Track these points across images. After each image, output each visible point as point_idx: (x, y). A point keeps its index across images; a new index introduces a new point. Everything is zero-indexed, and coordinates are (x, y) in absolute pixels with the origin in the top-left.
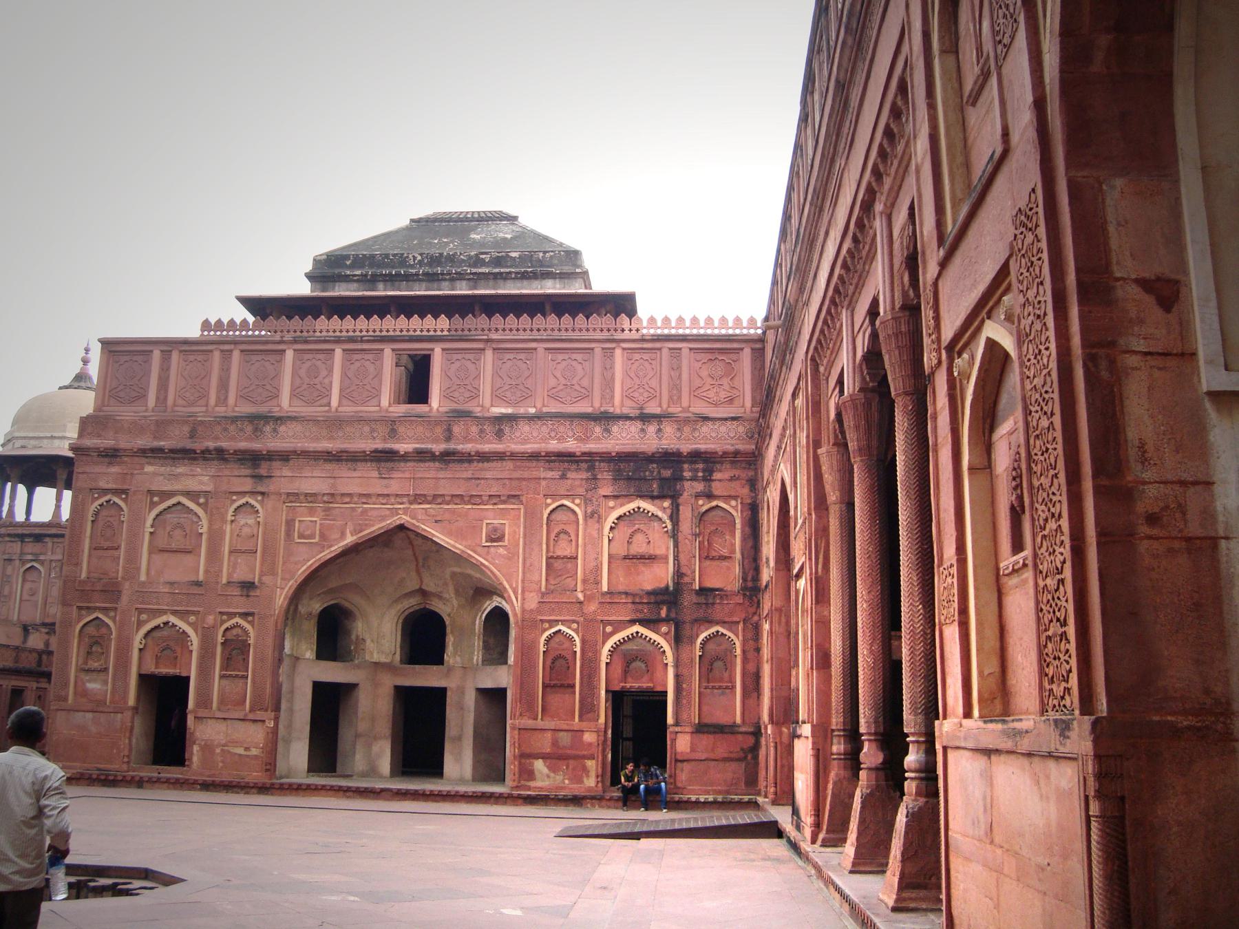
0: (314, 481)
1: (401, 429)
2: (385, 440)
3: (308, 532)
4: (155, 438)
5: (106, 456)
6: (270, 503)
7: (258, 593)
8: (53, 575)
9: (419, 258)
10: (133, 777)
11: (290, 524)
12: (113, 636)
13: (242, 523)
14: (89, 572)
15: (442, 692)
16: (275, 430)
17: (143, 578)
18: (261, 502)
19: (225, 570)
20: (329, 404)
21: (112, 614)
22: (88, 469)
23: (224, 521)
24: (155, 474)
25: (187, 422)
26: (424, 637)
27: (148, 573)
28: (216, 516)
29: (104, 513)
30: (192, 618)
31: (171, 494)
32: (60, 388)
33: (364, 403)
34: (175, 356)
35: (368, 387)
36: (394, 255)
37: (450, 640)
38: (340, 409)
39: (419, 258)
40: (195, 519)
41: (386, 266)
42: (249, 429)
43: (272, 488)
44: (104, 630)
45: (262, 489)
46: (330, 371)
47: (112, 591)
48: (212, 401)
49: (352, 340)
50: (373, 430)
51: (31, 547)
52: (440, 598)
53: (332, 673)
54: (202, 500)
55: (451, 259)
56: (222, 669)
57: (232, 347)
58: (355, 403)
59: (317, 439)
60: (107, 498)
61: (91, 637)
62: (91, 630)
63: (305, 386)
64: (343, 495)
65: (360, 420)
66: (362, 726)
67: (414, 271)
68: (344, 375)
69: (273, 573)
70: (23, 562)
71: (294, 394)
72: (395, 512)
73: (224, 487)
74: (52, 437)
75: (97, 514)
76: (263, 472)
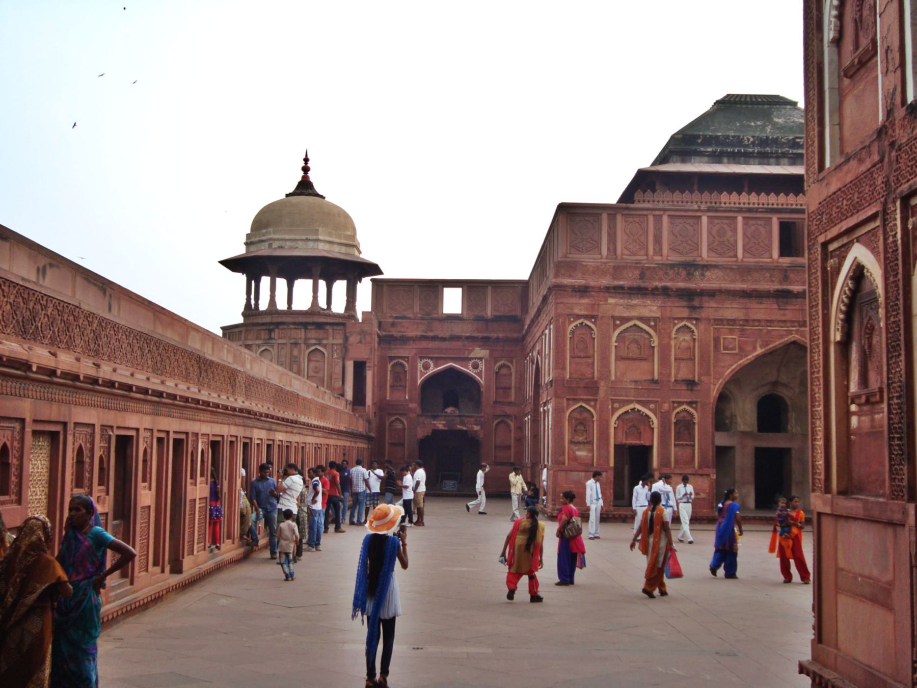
0: (732, 311)
1: (792, 276)
2: (781, 283)
3: (731, 346)
4: (614, 278)
5: (579, 291)
6: (702, 326)
7: (699, 388)
8: (335, 356)
9: (752, 140)
10: (620, 515)
11: (717, 340)
12: (595, 419)
13: (681, 339)
14: (571, 374)
15: (787, 451)
16: (702, 275)
17: (613, 378)
18: (696, 325)
19: (673, 371)
20: (736, 256)
21: (592, 403)
22: (565, 300)
23: (670, 337)
24: (616, 305)
25: (637, 268)
26: (772, 414)
27: (616, 375)
28: (664, 335)
29: (578, 332)
30: (652, 406)
31: (628, 319)
32: (287, 195)
33: (760, 256)
34: (619, 218)
35: (762, 244)
36: (733, 137)
37: (792, 416)
38: (745, 260)
39: (752, 140)
40: (647, 336)
41: (729, 145)
42: (684, 273)
43: (703, 315)
44: (585, 415)
45: (696, 316)
46: (735, 231)
47: (592, 387)
48: (651, 252)
49: (750, 210)
50: (771, 276)
51: (313, 334)
52: (785, 385)
53: (722, 440)
54: (652, 324)
55: (775, 141)
56: (675, 440)
57: (662, 213)
58: (754, 256)
59: (732, 281)
60: (581, 321)
61: (576, 419)
62: (575, 415)
63: (716, 243)
64: (754, 320)
65: (761, 268)
66: (738, 476)
67: (751, 150)
68: (745, 234)
69: (708, 374)
70: (308, 346)
71: (710, 249)
72: (789, 332)
73: (668, 314)
74: (307, 240)
75: (573, 332)
76: (696, 303)
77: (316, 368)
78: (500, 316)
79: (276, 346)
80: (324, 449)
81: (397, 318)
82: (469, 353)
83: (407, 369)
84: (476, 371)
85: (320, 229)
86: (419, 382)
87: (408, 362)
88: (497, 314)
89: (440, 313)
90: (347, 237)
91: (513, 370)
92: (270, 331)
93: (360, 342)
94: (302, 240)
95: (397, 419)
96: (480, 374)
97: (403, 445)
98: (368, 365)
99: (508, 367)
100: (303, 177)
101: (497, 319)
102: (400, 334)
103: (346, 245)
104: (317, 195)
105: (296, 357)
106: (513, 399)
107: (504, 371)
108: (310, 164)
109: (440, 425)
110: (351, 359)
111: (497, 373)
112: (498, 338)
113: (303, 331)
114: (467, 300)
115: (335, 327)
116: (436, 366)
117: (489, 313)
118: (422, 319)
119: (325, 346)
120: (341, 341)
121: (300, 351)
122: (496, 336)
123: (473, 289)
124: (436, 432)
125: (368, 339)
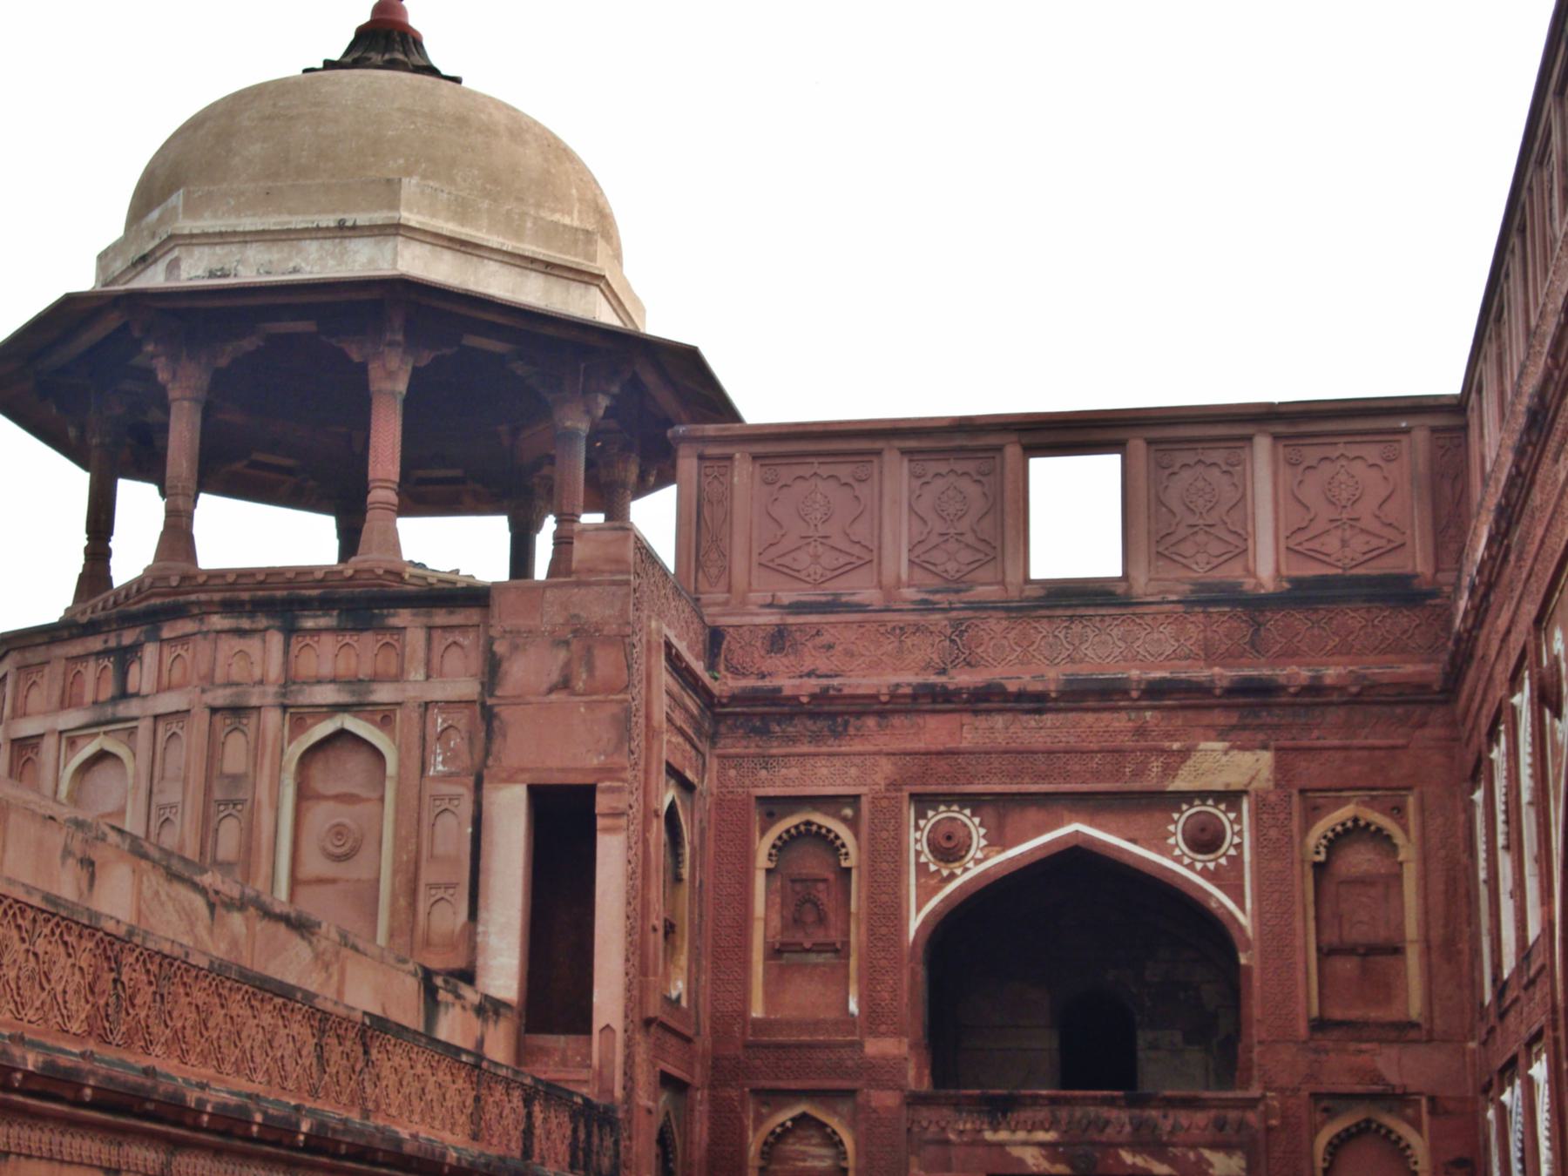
8: (438, 767)
51: (328, 655)
70: (299, 718)
77: (339, 831)
78: (1323, 581)
79: (144, 727)
81: (798, 608)
82: (1170, 771)
84: (1209, 861)
85: (410, 185)
86: (914, 923)
87: (853, 824)
88: (1312, 570)
89: (1013, 577)
90: (553, 232)
91: (1408, 852)
92: (125, 657)
94: (316, 233)
95: (802, 1120)
96: (1229, 879)
98: (602, 803)
99: (1380, 837)
101: (1305, 595)
102: (813, 685)
103: (549, 268)
104: (432, 71)
105: (236, 780)
106: (1415, 1007)
107: (1359, 860)
110: (510, 779)
112: (1315, 688)
113: (276, 640)
115: (441, 617)
116: (998, 840)
117: (1265, 568)
118: (926, 607)
119: (385, 716)
120: (467, 688)
121: (256, 754)
122: (1305, 675)
125: (606, 662)
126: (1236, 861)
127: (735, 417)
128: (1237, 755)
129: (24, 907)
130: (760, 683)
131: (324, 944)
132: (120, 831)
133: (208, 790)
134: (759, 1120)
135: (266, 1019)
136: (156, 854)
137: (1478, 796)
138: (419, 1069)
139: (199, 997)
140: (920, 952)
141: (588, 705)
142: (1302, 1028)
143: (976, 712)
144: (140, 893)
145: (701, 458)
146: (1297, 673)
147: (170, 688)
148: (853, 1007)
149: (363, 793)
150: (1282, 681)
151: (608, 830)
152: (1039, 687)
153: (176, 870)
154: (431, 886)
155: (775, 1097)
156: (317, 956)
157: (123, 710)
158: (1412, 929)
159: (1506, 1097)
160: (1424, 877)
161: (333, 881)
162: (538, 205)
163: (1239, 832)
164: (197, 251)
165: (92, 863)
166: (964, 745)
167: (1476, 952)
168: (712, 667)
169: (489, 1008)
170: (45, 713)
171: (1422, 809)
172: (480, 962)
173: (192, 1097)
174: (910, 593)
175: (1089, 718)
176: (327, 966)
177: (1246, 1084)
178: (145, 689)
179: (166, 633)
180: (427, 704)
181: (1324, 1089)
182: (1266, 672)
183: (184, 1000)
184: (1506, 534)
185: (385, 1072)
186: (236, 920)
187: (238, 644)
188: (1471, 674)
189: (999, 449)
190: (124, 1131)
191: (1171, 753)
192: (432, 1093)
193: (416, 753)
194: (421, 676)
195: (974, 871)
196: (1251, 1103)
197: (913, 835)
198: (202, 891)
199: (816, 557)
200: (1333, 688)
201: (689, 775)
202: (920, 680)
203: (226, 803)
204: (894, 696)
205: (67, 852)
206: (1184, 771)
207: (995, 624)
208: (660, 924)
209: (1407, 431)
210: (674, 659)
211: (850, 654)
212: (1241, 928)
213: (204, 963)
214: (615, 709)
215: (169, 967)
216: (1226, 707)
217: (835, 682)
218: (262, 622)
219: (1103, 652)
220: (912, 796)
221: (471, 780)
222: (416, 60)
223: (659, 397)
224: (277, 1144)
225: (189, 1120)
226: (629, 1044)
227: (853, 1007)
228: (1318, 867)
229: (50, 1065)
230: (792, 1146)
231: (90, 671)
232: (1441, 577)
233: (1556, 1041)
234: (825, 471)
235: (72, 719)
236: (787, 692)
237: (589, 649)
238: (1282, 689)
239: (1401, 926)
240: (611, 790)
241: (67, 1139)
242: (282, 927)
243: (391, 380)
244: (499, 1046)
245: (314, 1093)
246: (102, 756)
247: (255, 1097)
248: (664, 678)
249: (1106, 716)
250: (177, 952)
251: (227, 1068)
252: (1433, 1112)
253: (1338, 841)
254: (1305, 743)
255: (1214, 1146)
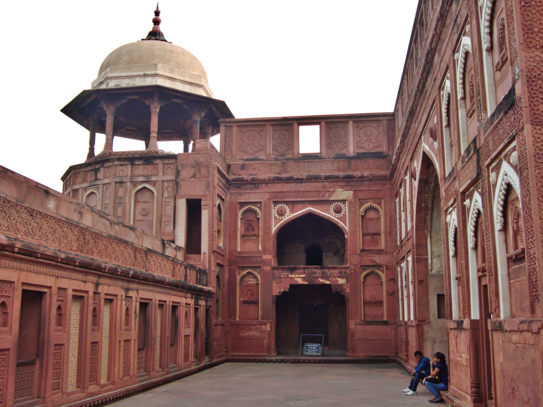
8: (166, 195)
51: (141, 170)
70: (135, 184)
77: (144, 209)
79: (101, 186)
80: (169, 310)
81: (247, 160)
82: (330, 196)
83: (260, 216)
84: (339, 215)
85: (160, 65)
86: (274, 229)
87: (260, 208)
88: (361, 151)
89: (296, 153)
90: (192, 76)
91: (382, 213)
92: (96, 171)
93: (194, 176)
95: (249, 273)
96: (343, 220)
97: (256, 303)
98: (203, 203)
99: (376, 209)
100: (153, 28)
101: (360, 156)
103: (191, 84)
104: (165, 41)
105: (121, 198)
107: (371, 215)
108: (161, 17)
109: (299, 279)
110: (182, 198)
111: (363, 217)
112: (362, 177)
113: (129, 167)
114: (326, 139)
115: (166, 161)
116: (292, 211)
117: (351, 150)
118: (276, 159)
119: (154, 184)
120: (172, 177)
121: (125, 193)
122: (360, 174)
123: (331, 125)
124: (294, 287)
125: (203, 171)
126: (345, 215)
127: (233, 117)
128: (345, 192)
129: (60, 220)
130: (239, 177)
131: (138, 233)
132: (88, 206)
133: (115, 200)
134: (239, 273)
135: (122, 248)
136: (97, 211)
137: (397, 200)
138: (159, 260)
139: (105, 243)
140: (275, 236)
141: (200, 181)
142: (359, 252)
143: (287, 183)
144: (93, 220)
145: (226, 126)
146: (358, 174)
147: (106, 178)
148: (260, 248)
149: (150, 201)
150: (355, 175)
151: (204, 209)
152: (301, 177)
153: (102, 215)
154: (165, 222)
155: (243, 268)
156: (136, 236)
157: (96, 183)
158: (382, 230)
159: (402, 265)
160: (385, 218)
161: (143, 221)
162: (189, 70)
163: (346, 209)
164: (112, 81)
165: (81, 213)
166: (285, 190)
167: (396, 234)
168: (228, 173)
169: (178, 248)
170: (79, 184)
171: (385, 204)
172: (176, 238)
173: (103, 265)
174: (272, 156)
175: (313, 184)
176: (139, 238)
177: (346, 264)
178: (101, 178)
179: (105, 166)
180: (163, 181)
181: (363, 264)
182: (351, 173)
183: (101, 243)
184: (404, 141)
185: (151, 260)
186: (117, 227)
187: (121, 168)
188: (396, 173)
189: (293, 124)
190: (87, 273)
191: (331, 191)
192: (163, 266)
193: (161, 192)
194: (162, 175)
195: (287, 218)
196: (347, 268)
197: (273, 210)
198: (109, 220)
199: (251, 149)
200: (366, 177)
201: (223, 197)
202: (275, 176)
203: (119, 203)
204: (269, 180)
205: (75, 210)
206: (333, 195)
207: (292, 163)
208: (216, 230)
209: (382, 120)
210: (219, 171)
211: (259, 170)
212: (346, 230)
213: (106, 235)
214: (206, 182)
215: (97, 236)
216: (343, 181)
217: (256, 176)
218: (126, 163)
219: (316, 169)
220: (273, 202)
221: (173, 198)
222: (162, 39)
223: (216, 113)
224: (125, 276)
225: (103, 271)
226: (209, 256)
227: (260, 248)
228: (362, 216)
229: (68, 257)
230: (246, 279)
231: (89, 174)
232: (389, 152)
233: (414, 252)
234: (253, 129)
235: (85, 185)
236: (245, 179)
237: (199, 168)
238: (355, 177)
239: (380, 229)
240: (204, 200)
241: (73, 274)
242: (128, 229)
243: (155, 109)
244: (180, 256)
245: (134, 265)
246: (92, 193)
247: (119, 266)
248: (217, 175)
249: (316, 183)
250: (99, 232)
251: (112, 259)
252: (386, 269)
253: (366, 211)
254: (360, 189)
255: (339, 277)
